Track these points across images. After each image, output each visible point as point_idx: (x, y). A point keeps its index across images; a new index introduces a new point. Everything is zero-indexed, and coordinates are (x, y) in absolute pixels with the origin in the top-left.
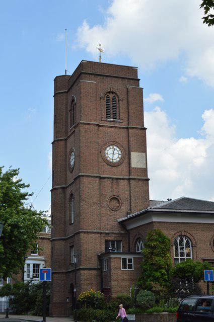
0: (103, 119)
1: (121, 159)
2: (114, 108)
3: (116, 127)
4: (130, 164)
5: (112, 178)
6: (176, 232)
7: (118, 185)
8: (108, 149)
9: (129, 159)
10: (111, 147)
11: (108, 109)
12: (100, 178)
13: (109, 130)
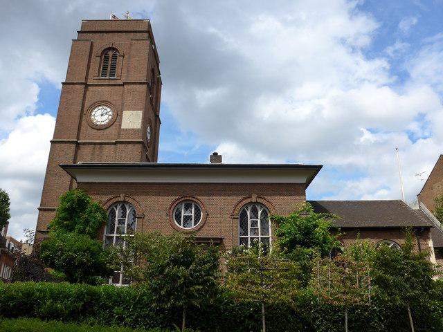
0: (95, 78)
1: (110, 120)
2: (114, 65)
3: (109, 85)
4: (120, 125)
5: (95, 144)
6: (111, 196)
7: (101, 151)
8: (96, 109)
9: (121, 119)
10: (101, 108)
11: (105, 67)
12: (78, 144)
13: (100, 89)
